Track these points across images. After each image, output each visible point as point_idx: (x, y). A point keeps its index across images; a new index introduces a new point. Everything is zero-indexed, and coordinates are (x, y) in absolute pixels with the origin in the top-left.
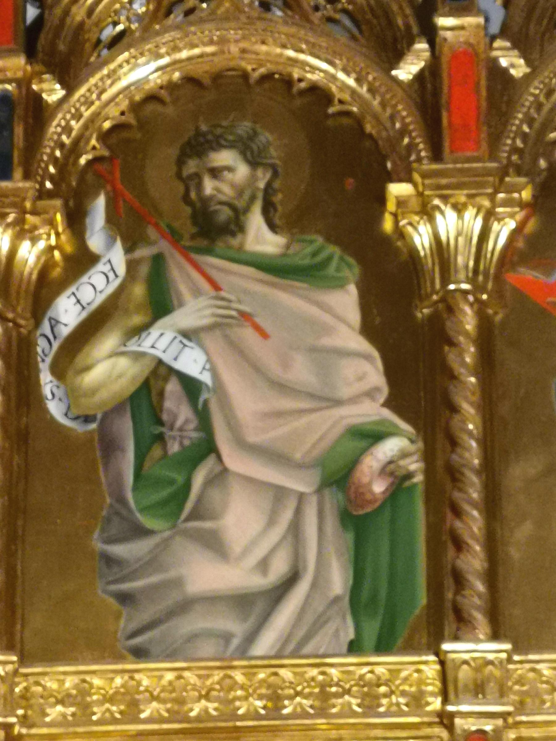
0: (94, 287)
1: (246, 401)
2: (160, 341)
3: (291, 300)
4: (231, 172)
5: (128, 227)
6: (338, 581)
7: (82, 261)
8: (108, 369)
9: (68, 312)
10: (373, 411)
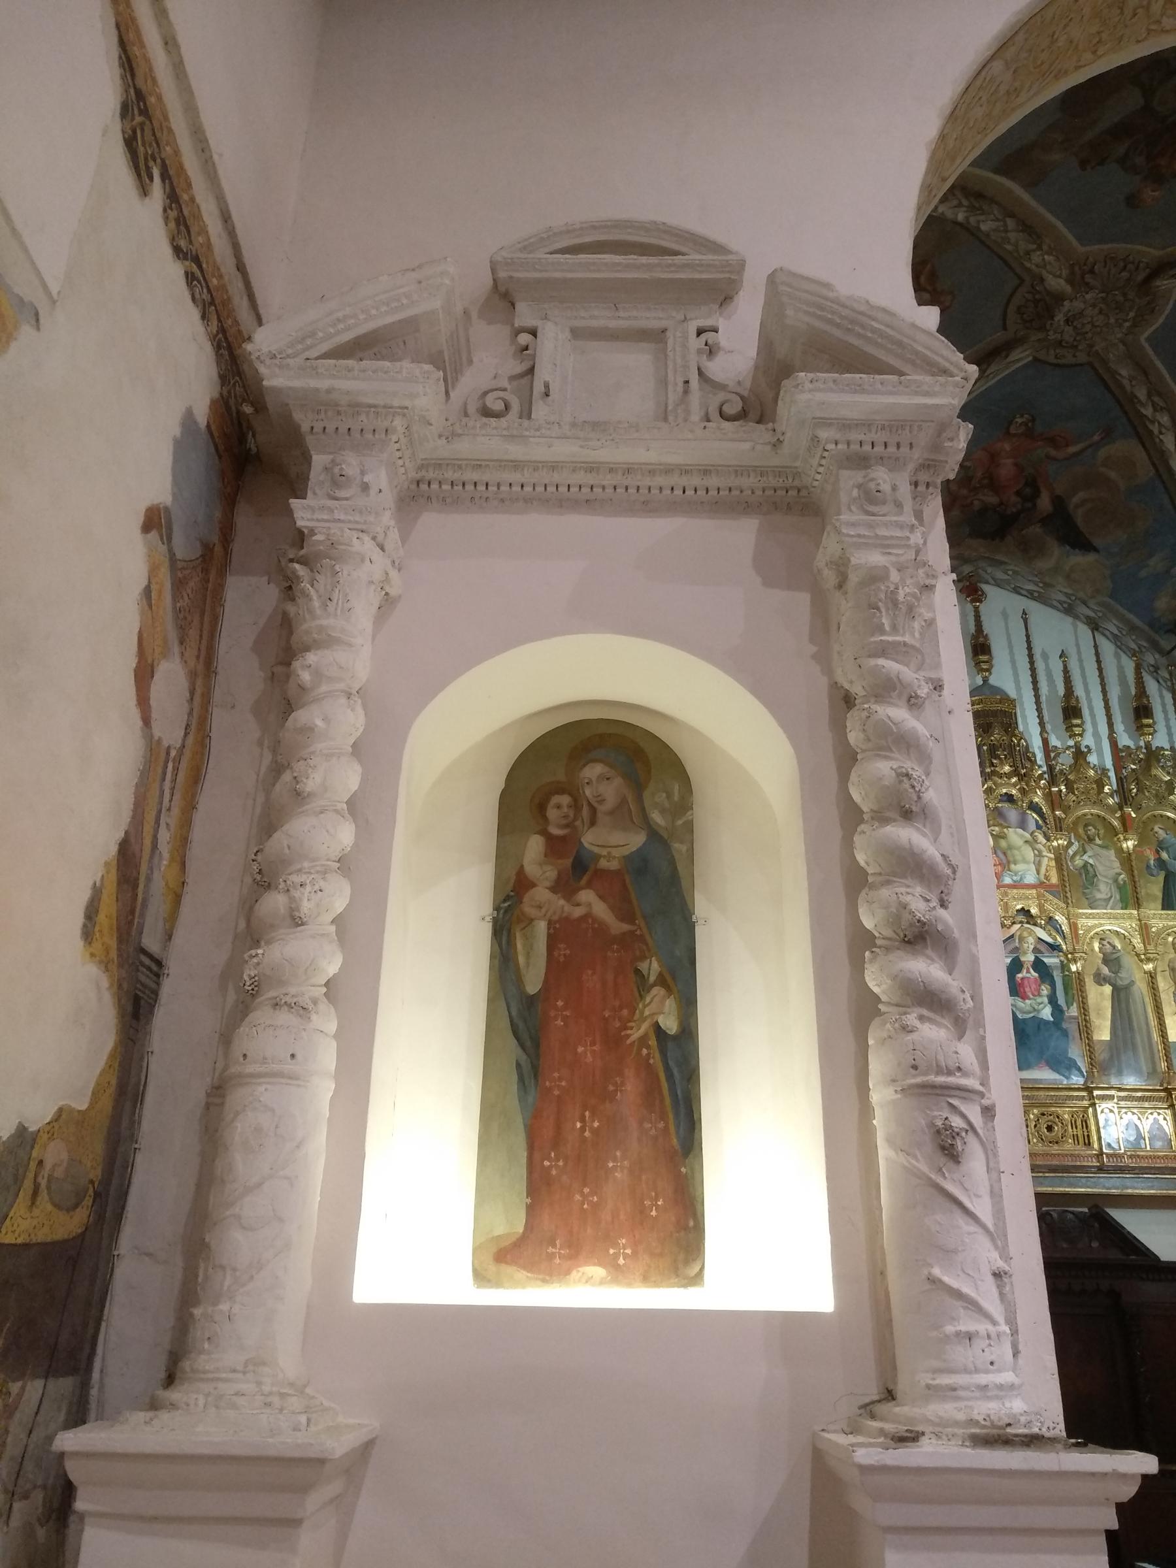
0: (1074, 848)
1: (1100, 869)
2: (1085, 857)
3: (1104, 852)
4: (1092, 830)
5: (1078, 837)
6: (1118, 897)
7: (1070, 844)
8: (1078, 862)
9: (1071, 852)
10: (1119, 870)
